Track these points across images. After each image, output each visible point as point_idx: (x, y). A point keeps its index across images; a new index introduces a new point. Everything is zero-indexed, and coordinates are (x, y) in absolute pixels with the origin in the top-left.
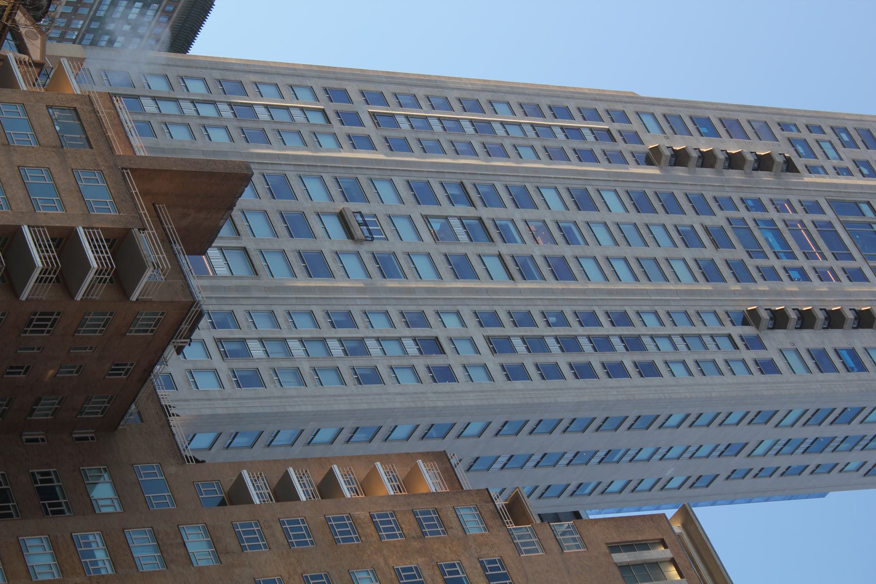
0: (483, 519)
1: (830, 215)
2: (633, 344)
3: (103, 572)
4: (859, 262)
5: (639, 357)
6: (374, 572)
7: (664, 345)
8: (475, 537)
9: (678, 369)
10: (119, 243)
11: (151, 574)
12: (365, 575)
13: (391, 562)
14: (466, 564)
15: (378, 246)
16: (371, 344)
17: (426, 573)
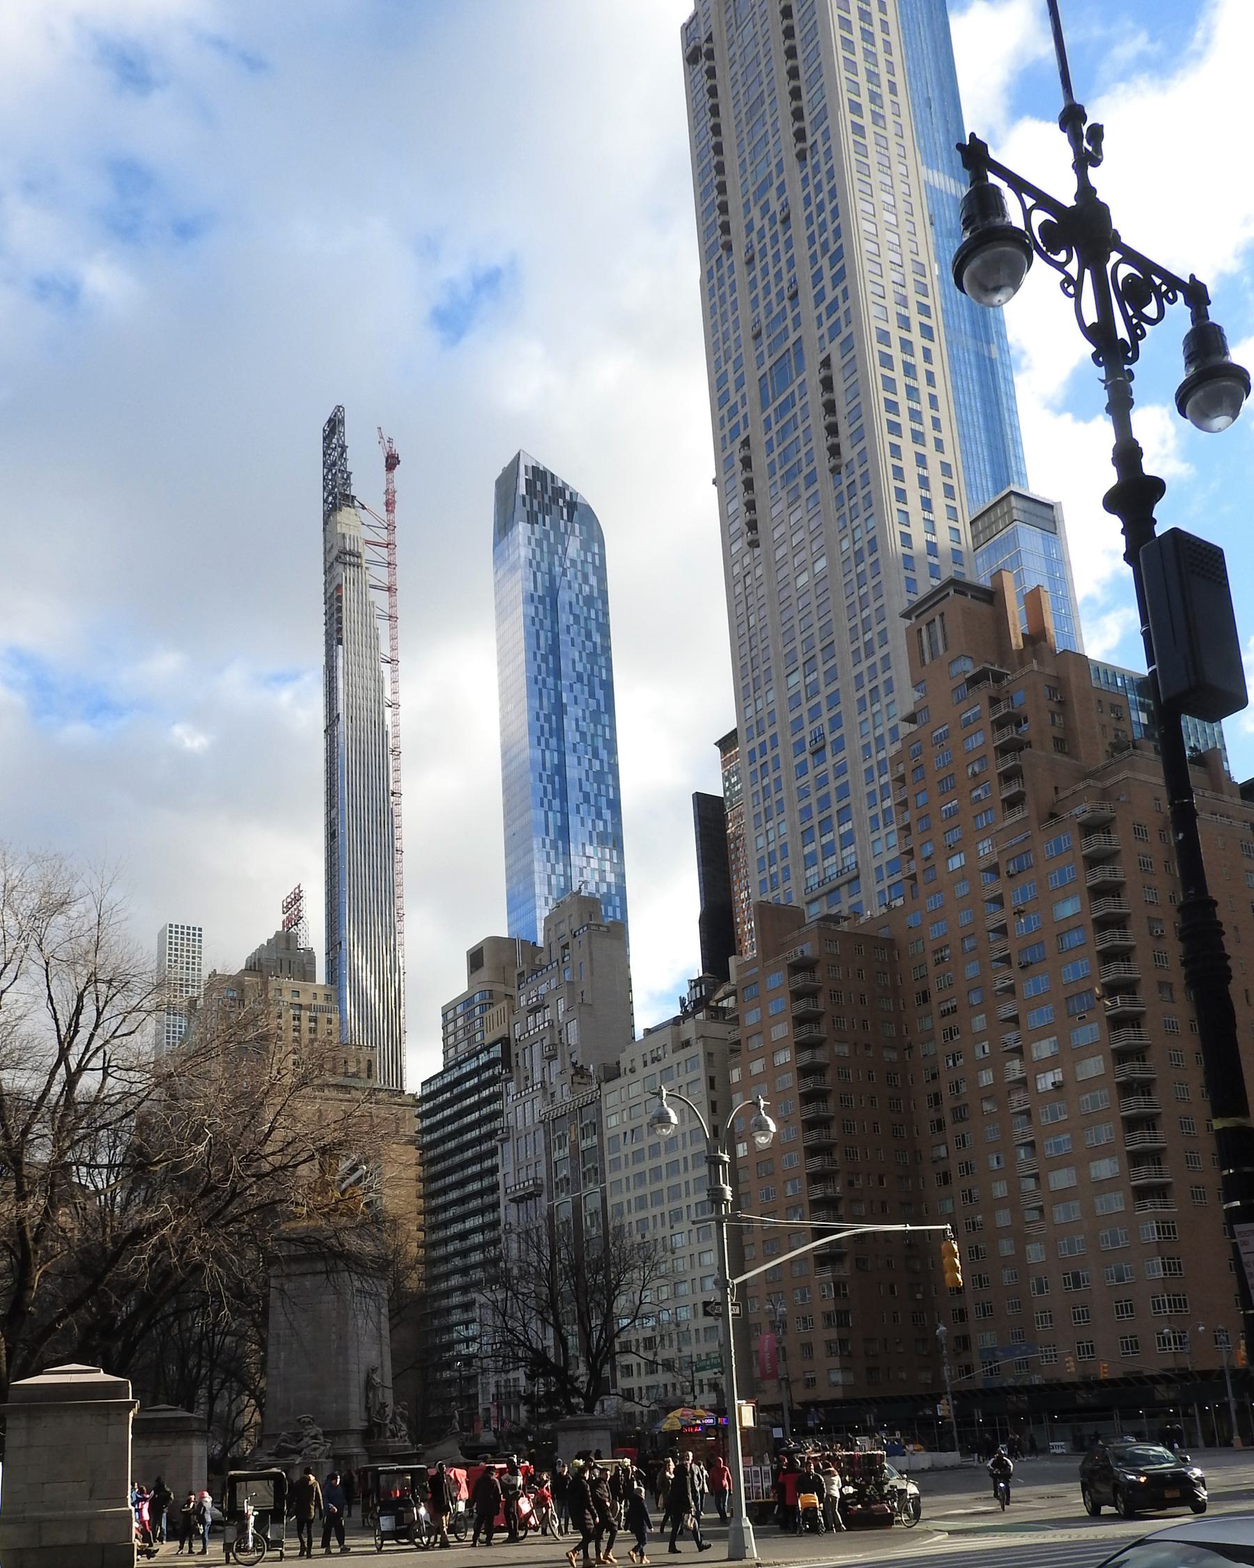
1: (770, 410)
2: (859, 555)
4: (794, 387)
5: (866, 554)
7: (858, 534)
9: (871, 524)
10: (797, 968)
15: (827, 731)
16: (878, 733)
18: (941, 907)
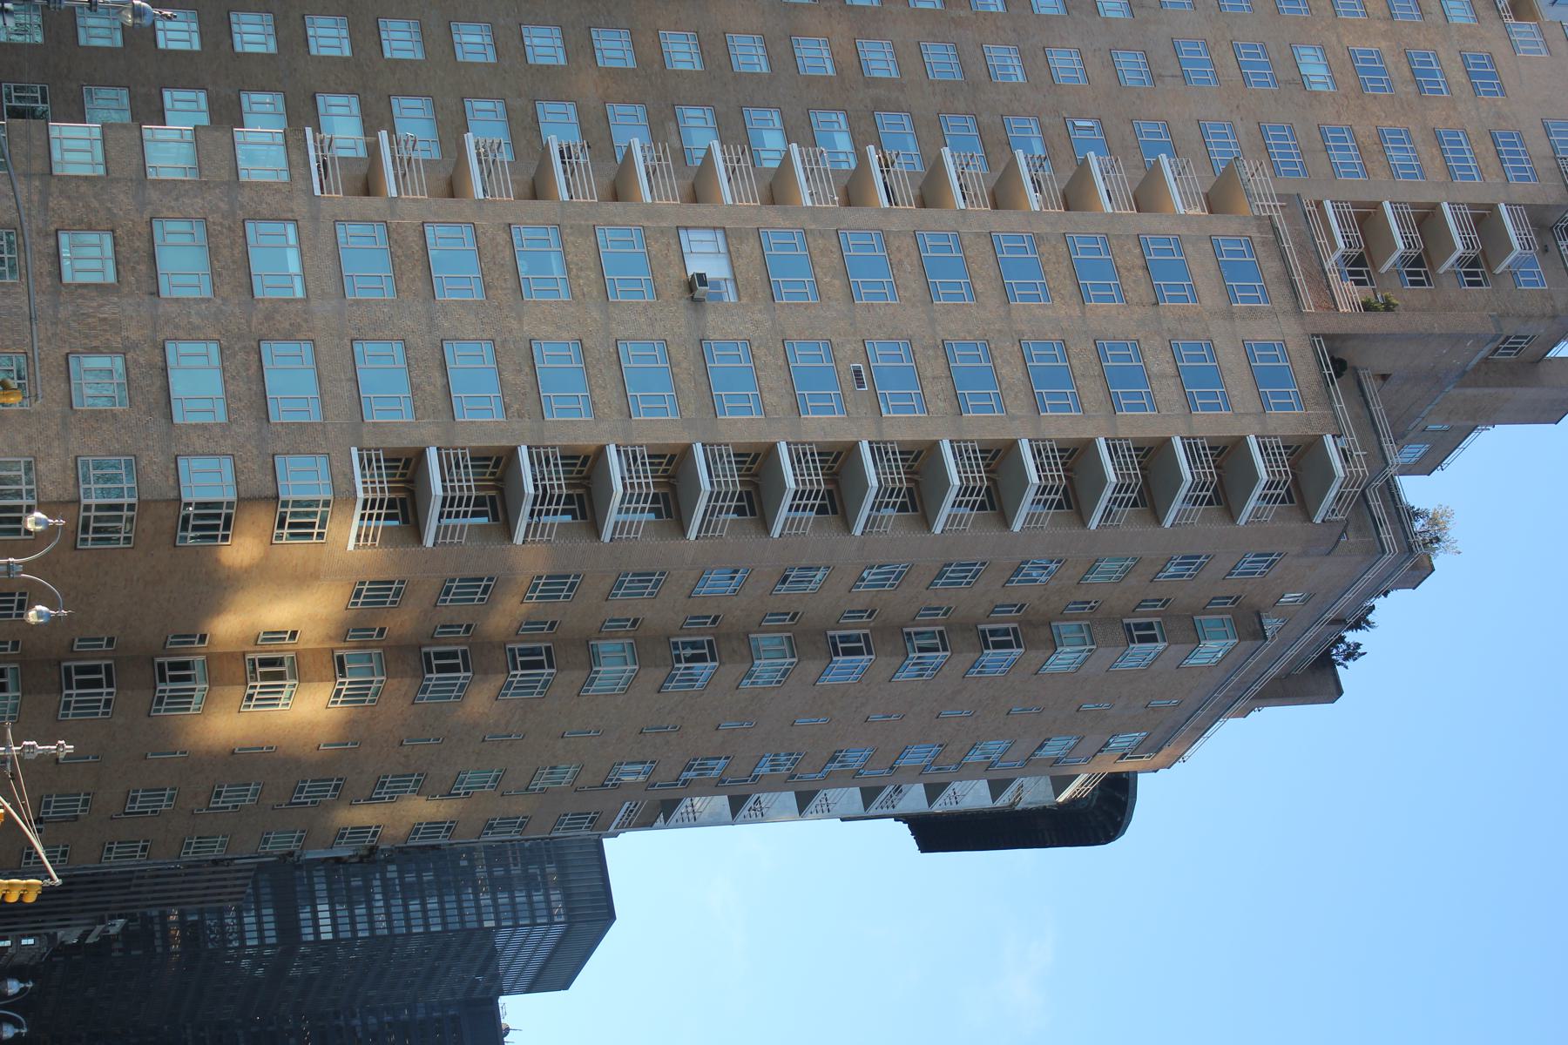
0: (1474, 10)
3: (993, 9)
6: (1323, 49)
8: (1459, 27)
11: (1049, 18)
12: (1311, 52)
13: (1346, 42)
14: (1442, 55)
17: (1389, 60)
18: (1184, 76)
